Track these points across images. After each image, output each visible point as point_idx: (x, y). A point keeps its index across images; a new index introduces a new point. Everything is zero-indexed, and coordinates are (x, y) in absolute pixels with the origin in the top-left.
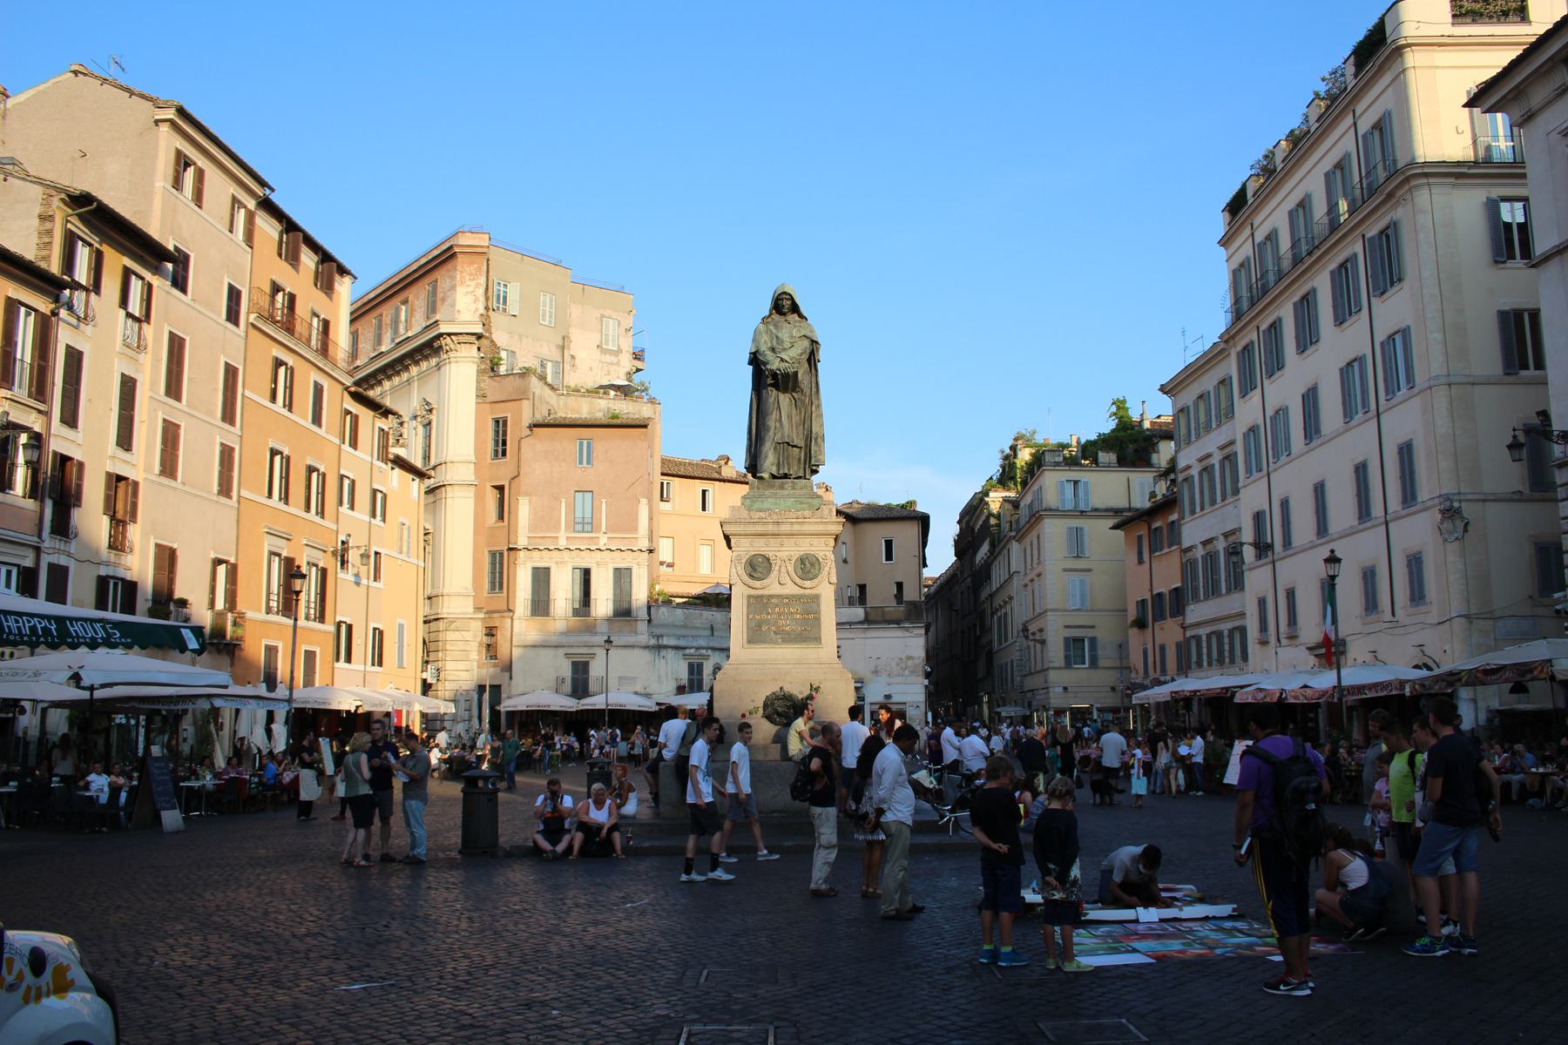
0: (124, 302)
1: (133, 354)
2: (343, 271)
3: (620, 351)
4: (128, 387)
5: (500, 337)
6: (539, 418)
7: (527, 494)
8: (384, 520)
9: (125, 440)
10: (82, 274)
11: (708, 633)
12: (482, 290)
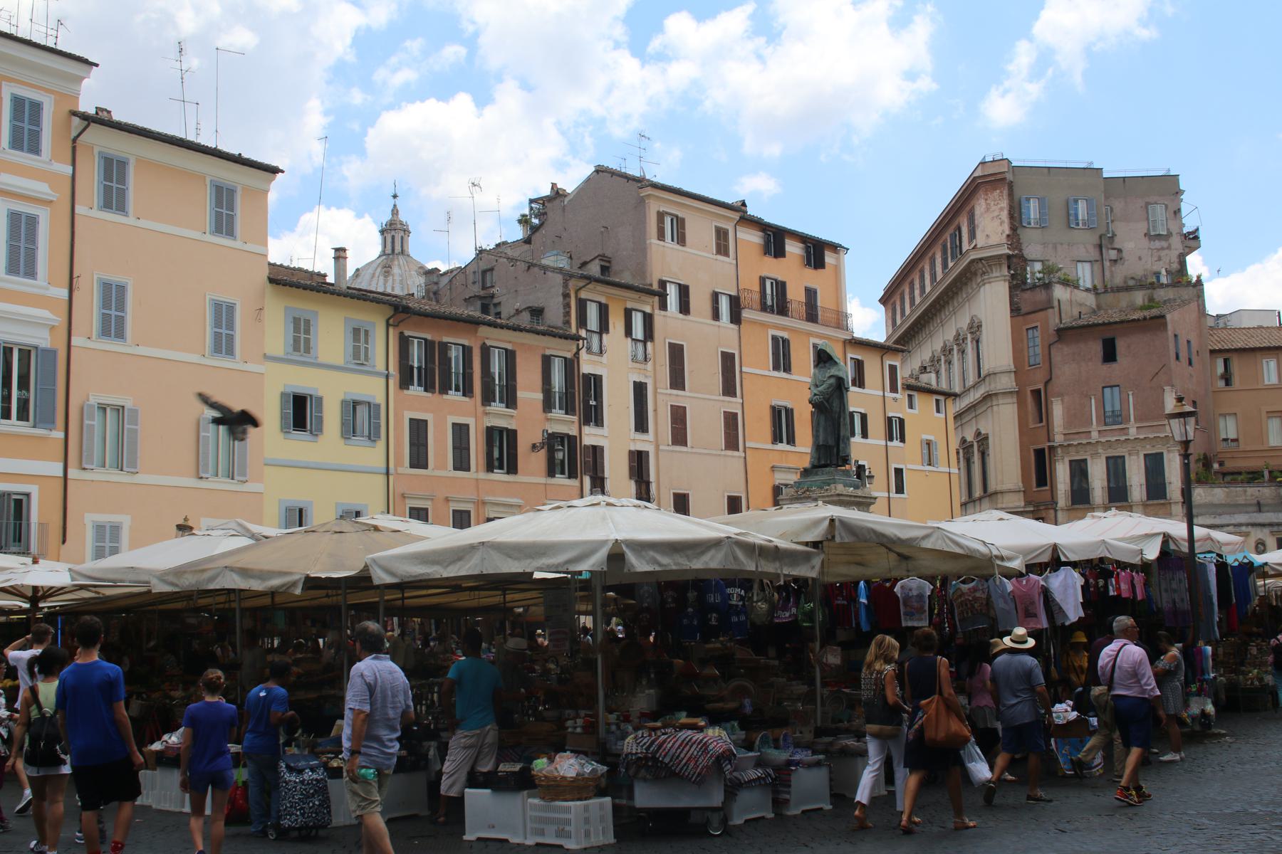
0: (628, 332)
1: (642, 366)
2: (835, 248)
3: (1169, 235)
4: (640, 389)
5: (1031, 251)
6: (1067, 321)
7: (1060, 395)
8: (903, 440)
9: (641, 425)
10: (593, 322)
11: (1255, 508)
12: (1005, 215)
